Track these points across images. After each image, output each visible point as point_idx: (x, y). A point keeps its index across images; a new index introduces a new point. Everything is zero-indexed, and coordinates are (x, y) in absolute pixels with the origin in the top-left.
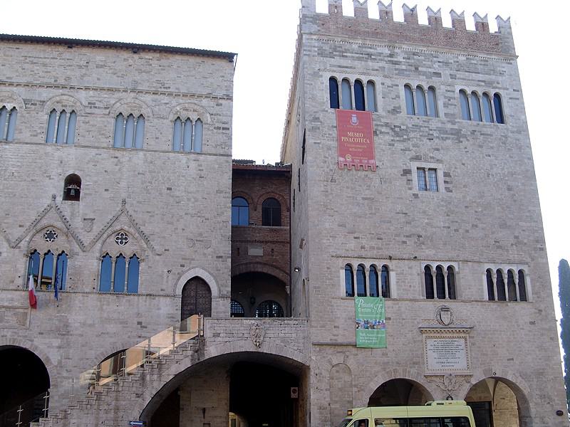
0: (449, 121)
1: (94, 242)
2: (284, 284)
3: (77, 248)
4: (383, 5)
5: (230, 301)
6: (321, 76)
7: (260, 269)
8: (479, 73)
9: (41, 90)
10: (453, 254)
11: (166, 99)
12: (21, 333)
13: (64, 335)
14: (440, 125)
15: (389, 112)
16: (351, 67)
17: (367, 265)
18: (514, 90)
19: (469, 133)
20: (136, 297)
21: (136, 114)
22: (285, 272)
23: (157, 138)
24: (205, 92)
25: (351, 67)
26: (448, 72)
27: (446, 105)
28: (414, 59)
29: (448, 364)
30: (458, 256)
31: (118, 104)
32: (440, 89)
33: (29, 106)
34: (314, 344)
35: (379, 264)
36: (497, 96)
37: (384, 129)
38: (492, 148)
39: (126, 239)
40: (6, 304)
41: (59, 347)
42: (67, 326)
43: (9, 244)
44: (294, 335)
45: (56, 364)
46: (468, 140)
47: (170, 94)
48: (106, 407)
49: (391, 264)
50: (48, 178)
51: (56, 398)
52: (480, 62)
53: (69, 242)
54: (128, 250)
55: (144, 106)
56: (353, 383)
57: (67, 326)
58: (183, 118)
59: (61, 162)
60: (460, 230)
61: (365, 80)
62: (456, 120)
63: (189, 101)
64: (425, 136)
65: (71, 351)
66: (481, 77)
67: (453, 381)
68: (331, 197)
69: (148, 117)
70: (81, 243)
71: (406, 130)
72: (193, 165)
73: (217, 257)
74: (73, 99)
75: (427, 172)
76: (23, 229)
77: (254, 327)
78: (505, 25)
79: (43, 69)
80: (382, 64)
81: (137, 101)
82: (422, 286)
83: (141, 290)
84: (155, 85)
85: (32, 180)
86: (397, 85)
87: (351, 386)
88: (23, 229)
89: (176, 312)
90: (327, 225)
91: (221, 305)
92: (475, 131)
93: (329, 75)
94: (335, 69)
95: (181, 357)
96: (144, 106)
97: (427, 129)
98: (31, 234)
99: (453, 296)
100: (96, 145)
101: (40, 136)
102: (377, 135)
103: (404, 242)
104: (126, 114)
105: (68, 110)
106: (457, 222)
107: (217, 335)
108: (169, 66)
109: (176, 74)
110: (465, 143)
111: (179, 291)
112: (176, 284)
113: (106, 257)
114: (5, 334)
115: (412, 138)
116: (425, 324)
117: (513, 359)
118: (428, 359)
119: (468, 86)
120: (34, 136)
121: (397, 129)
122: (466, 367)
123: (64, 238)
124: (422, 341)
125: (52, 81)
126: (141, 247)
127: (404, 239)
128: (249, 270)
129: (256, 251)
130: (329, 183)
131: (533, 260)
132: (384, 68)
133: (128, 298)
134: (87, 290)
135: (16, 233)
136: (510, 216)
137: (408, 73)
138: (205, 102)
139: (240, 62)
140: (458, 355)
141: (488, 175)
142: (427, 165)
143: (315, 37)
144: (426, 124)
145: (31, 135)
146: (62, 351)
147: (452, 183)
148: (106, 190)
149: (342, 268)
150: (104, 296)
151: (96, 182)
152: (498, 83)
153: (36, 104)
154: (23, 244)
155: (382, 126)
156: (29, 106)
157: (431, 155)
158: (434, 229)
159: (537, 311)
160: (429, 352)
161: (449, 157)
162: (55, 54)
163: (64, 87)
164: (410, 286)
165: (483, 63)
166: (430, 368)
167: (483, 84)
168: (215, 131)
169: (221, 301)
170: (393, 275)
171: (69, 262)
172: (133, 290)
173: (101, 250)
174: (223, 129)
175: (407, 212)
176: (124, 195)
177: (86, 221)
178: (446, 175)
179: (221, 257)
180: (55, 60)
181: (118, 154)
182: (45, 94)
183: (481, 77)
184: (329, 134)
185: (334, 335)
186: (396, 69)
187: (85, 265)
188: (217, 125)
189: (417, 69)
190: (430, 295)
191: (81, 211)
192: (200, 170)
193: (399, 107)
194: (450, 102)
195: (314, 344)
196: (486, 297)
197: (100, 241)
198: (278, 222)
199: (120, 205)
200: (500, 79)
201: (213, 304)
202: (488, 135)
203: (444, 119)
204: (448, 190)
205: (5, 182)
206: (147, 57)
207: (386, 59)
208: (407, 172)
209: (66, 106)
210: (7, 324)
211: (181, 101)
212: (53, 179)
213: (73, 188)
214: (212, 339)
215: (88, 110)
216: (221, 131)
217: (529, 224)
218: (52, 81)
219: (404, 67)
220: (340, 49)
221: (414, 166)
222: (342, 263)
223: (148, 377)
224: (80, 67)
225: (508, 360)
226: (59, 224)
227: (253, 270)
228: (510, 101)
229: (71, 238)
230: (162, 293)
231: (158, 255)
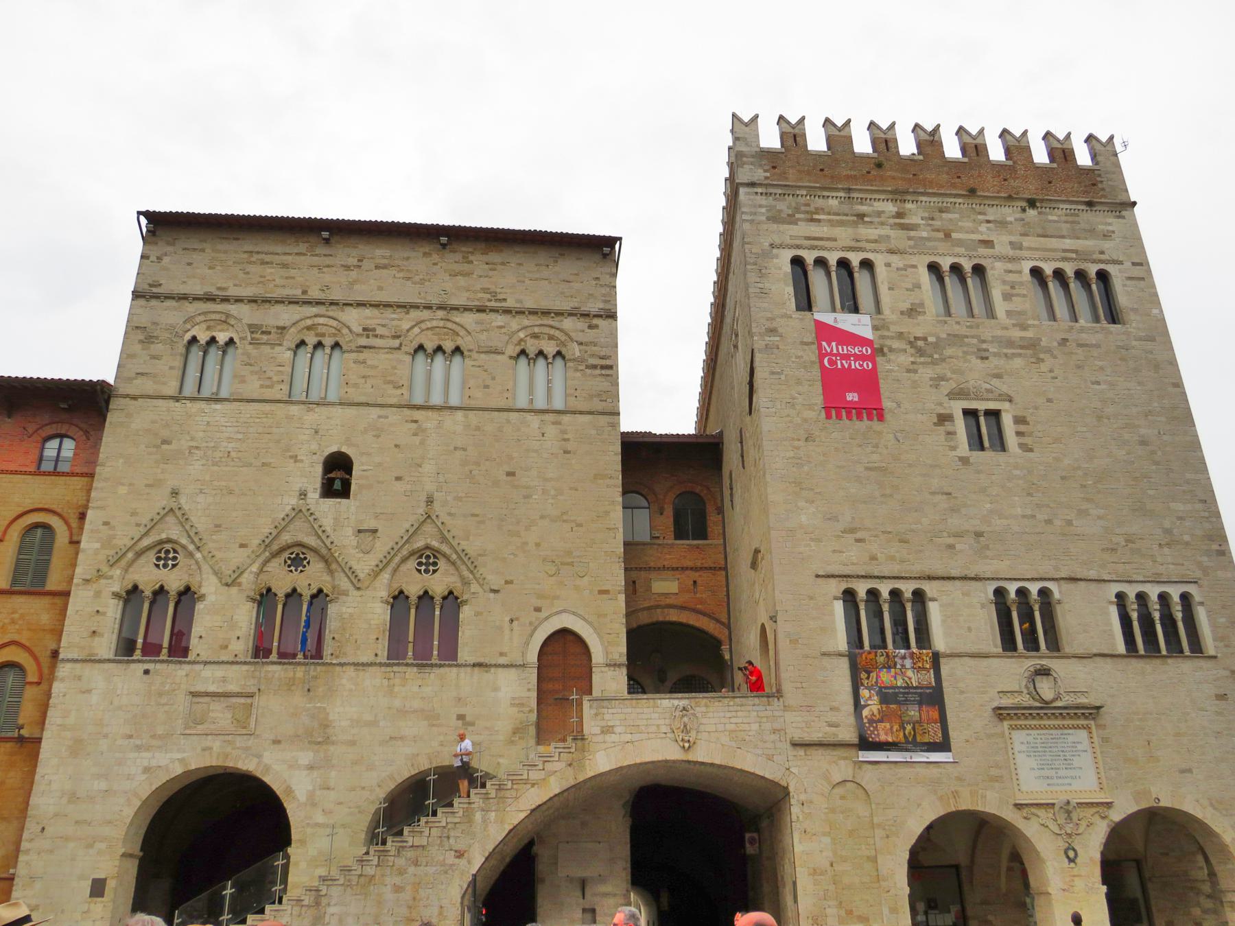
0: (1014, 325)
1: (376, 573)
2: (716, 644)
3: (344, 583)
4: (879, 128)
5: (624, 671)
6: (777, 257)
7: (674, 616)
8: (1063, 237)
9: (279, 307)
10: (1046, 568)
11: (500, 320)
12: (240, 742)
14: (999, 333)
15: (902, 313)
16: (828, 239)
17: (885, 589)
18: (1133, 264)
19: (1055, 344)
20: (455, 670)
21: (449, 346)
22: (718, 621)
23: (487, 387)
24: (566, 306)
25: (828, 239)
26: (1006, 239)
27: (1007, 297)
28: (941, 219)
29: (1060, 781)
30: (1057, 569)
31: (416, 330)
32: (993, 268)
33: (257, 336)
34: (795, 745)
35: (907, 588)
36: (1103, 276)
37: (896, 344)
38: (1102, 368)
39: (435, 564)
41: (311, 768)
42: (325, 726)
43: (220, 580)
44: (755, 727)
46: (1055, 357)
47: (507, 311)
48: (397, 880)
49: (929, 588)
51: (303, 865)
52: (1064, 218)
53: (331, 572)
54: (439, 583)
55: (462, 333)
56: (876, 820)
57: (327, 726)
58: (532, 351)
59: (316, 432)
60: (1057, 522)
61: (855, 259)
62: (1030, 322)
63: (540, 322)
64: (973, 353)
65: (333, 774)
66: (1068, 243)
67: (1074, 816)
68: (806, 468)
69: (470, 351)
70: (352, 574)
71: (936, 345)
72: (551, 431)
73: (601, 592)
74: (334, 323)
75: (982, 419)
77: (678, 713)
78: (1103, 149)
79: (283, 272)
80: (885, 231)
81: (449, 325)
82: (992, 628)
83: (464, 655)
84: (480, 295)
85: (264, 464)
86: (914, 266)
87: (873, 826)
89: (528, 694)
90: (804, 518)
91: (610, 679)
92: (1065, 340)
93: (788, 255)
94: (798, 242)
95: (542, 775)
96: (462, 333)
97: (975, 341)
98: (261, 560)
99: (1054, 644)
100: (380, 401)
101: (278, 387)
102: (884, 355)
103: (951, 547)
104: (430, 346)
105: (328, 342)
106: (1048, 506)
107: (608, 730)
108: (503, 264)
109: (519, 281)
110: (1049, 362)
111: (533, 657)
112: (527, 643)
113: (398, 598)
114: (208, 744)
115: (950, 357)
116: (1006, 701)
117: (1190, 771)
118: (1019, 771)
119: (1045, 260)
120: (267, 387)
121: (920, 343)
122: (1096, 787)
123: (321, 565)
124: (1003, 733)
125: (299, 292)
126: (462, 578)
127: (951, 541)
128: (655, 620)
129: (665, 586)
130: (802, 443)
131: (1205, 571)
132: (888, 237)
133: (437, 671)
134: (364, 659)
135: (237, 557)
136: (1150, 492)
137: (931, 244)
138: (568, 323)
139: (627, 256)
140: (1076, 762)
141: (1099, 418)
142: (981, 406)
143: (760, 190)
144: (974, 332)
145: (262, 386)
146: (315, 773)
147: (1031, 434)
148: (398, 479)
149: (836, 598)
150: (396, 669)
151: (380, 464)
152: (1102, 253)
153: (270, 333)
154: (247, 579)
155: (892, 338)
156: (257, 336)
157: (988, 386)
158: (1005, 522)
159: (1227, 673)
160: (1020, 758)
161: (1019, 388)
162: (302, 247)
163: (319, 303)
164: (970, 629)
165: (1070, 219)
166: (1024, 788)
167: (1074, 256)
168: (589, 371)
169: (610, 673)
170: (934, 611)
171: (332, 609)
172: (450, 653)
173: (390, 585)
174: (603, 367)
175: (950, 490)
176: (430, 487)
177: (362, 535)
178: (1019, 420)
179: (606, 592)
180: (303, 258)
181: (418, 415)
182: (285, 315)
183: (1068, 243)
184: (797, 357)
185: (830, 725)
186: (910, 238)
187: (361, 616)
188: (592, 361)
189: (948, 236)
190: (1008, 642)
191: (353, 518)
192: (565, 440)
193: (922, 305)
194: (1014, 292)
195: (795, 745)
196: (1121, 648)
197: (389, 569)
198: (701, 532)
199: (423, 504)
200: (1106, 245)
201: (596, 678)
202: (1087, 345)
203: (1008, 322)
204: (1025, 448)
205: (216, 468)
206: (464, 249)
207: (892, 221)
208: (944, 419)
209: (323, 335)
210: (212, 727)
211: (526, 322)
212: (302, 461)
213: (338, 475)
214: (600, 738)
215: (363, 341)
216: (598, 372)
217: (1189, 507)
218: (299, 292)
219: (925, 234)
220: (807, 208)
221: (957, 408)
222: (837, 587)
223: (478, 816)
224: (347, 268)
225: (1183, 771)
226: (311, 541)
227: (661, 619)
228: (1129, 282)
230: (502, 660)
231: (495, 591)
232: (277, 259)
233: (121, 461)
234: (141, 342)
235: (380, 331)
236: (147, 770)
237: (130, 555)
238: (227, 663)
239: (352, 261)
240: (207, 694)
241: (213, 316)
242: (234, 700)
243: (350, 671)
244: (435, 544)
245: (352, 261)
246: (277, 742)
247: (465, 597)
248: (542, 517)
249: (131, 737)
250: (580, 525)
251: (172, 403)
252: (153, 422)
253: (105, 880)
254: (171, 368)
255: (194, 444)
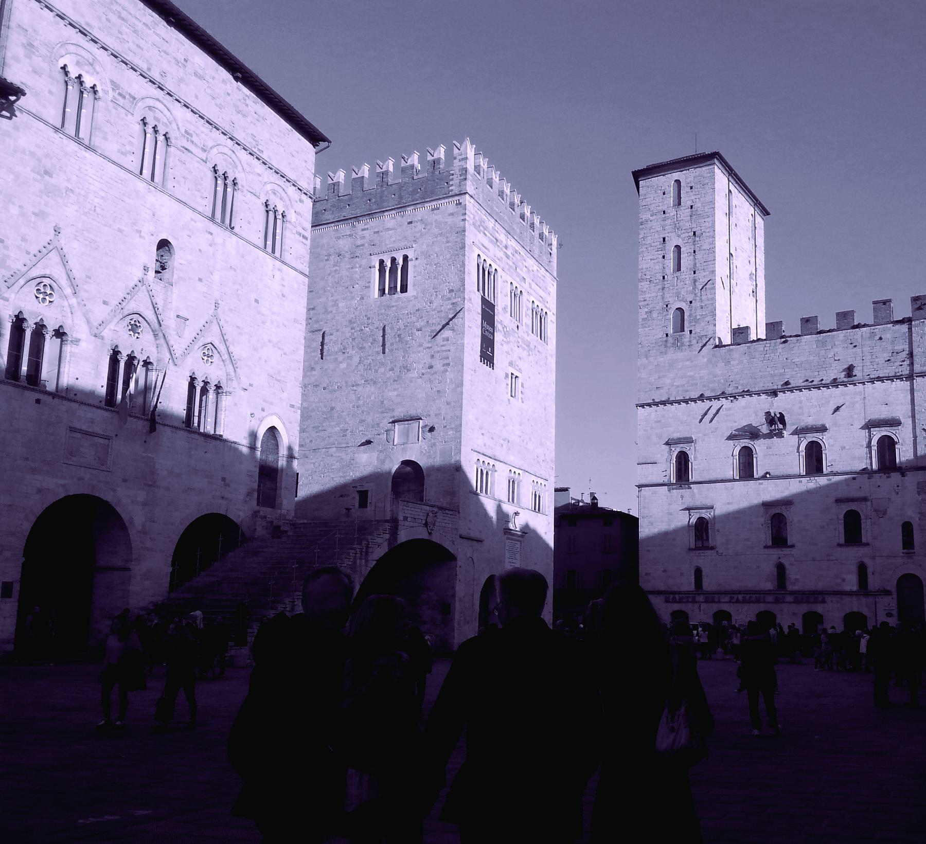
13: (150, 486)
40: (84, 427)
41: (145, 504)
45: (140, 528)
50: (138, 235)
76: (108, 309)
81: (233, 156)
88: (108, 309)
96: (240, 168)
123: (150, 336)
135: (100, 312)
148: (200, 280)
212: (143, 238)
216: (301, 238)
226: (150, 315)
229: (162, 341)
232: (132, 20)
233: (12, 176)
234: (23, 45)
235: (195, 139)
236: (39, 491)
237: (22, 282)
238: (94, 406)
239: (181, 58)
240: (81, 431)
241: (84, 53)
242: (97, 440)
243: (168, 429)
244: (216, 343)
245: (181, 58)
246: (125, 481)
247: (228, 390)
248: (270, 341)
249: (27, 459)
250: (285, 354)
251: (51, 132)
252: (37, 146)
253: (12, 583)
254: (50, 92)
255: (70, 186)
